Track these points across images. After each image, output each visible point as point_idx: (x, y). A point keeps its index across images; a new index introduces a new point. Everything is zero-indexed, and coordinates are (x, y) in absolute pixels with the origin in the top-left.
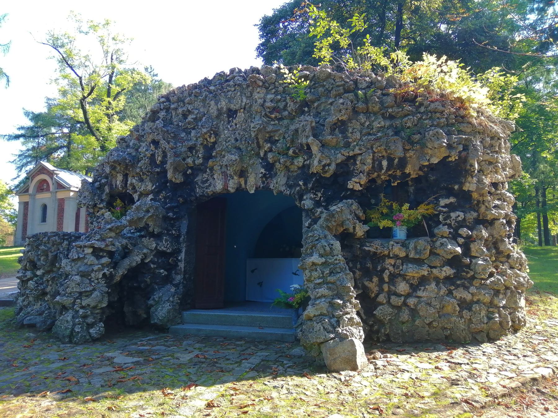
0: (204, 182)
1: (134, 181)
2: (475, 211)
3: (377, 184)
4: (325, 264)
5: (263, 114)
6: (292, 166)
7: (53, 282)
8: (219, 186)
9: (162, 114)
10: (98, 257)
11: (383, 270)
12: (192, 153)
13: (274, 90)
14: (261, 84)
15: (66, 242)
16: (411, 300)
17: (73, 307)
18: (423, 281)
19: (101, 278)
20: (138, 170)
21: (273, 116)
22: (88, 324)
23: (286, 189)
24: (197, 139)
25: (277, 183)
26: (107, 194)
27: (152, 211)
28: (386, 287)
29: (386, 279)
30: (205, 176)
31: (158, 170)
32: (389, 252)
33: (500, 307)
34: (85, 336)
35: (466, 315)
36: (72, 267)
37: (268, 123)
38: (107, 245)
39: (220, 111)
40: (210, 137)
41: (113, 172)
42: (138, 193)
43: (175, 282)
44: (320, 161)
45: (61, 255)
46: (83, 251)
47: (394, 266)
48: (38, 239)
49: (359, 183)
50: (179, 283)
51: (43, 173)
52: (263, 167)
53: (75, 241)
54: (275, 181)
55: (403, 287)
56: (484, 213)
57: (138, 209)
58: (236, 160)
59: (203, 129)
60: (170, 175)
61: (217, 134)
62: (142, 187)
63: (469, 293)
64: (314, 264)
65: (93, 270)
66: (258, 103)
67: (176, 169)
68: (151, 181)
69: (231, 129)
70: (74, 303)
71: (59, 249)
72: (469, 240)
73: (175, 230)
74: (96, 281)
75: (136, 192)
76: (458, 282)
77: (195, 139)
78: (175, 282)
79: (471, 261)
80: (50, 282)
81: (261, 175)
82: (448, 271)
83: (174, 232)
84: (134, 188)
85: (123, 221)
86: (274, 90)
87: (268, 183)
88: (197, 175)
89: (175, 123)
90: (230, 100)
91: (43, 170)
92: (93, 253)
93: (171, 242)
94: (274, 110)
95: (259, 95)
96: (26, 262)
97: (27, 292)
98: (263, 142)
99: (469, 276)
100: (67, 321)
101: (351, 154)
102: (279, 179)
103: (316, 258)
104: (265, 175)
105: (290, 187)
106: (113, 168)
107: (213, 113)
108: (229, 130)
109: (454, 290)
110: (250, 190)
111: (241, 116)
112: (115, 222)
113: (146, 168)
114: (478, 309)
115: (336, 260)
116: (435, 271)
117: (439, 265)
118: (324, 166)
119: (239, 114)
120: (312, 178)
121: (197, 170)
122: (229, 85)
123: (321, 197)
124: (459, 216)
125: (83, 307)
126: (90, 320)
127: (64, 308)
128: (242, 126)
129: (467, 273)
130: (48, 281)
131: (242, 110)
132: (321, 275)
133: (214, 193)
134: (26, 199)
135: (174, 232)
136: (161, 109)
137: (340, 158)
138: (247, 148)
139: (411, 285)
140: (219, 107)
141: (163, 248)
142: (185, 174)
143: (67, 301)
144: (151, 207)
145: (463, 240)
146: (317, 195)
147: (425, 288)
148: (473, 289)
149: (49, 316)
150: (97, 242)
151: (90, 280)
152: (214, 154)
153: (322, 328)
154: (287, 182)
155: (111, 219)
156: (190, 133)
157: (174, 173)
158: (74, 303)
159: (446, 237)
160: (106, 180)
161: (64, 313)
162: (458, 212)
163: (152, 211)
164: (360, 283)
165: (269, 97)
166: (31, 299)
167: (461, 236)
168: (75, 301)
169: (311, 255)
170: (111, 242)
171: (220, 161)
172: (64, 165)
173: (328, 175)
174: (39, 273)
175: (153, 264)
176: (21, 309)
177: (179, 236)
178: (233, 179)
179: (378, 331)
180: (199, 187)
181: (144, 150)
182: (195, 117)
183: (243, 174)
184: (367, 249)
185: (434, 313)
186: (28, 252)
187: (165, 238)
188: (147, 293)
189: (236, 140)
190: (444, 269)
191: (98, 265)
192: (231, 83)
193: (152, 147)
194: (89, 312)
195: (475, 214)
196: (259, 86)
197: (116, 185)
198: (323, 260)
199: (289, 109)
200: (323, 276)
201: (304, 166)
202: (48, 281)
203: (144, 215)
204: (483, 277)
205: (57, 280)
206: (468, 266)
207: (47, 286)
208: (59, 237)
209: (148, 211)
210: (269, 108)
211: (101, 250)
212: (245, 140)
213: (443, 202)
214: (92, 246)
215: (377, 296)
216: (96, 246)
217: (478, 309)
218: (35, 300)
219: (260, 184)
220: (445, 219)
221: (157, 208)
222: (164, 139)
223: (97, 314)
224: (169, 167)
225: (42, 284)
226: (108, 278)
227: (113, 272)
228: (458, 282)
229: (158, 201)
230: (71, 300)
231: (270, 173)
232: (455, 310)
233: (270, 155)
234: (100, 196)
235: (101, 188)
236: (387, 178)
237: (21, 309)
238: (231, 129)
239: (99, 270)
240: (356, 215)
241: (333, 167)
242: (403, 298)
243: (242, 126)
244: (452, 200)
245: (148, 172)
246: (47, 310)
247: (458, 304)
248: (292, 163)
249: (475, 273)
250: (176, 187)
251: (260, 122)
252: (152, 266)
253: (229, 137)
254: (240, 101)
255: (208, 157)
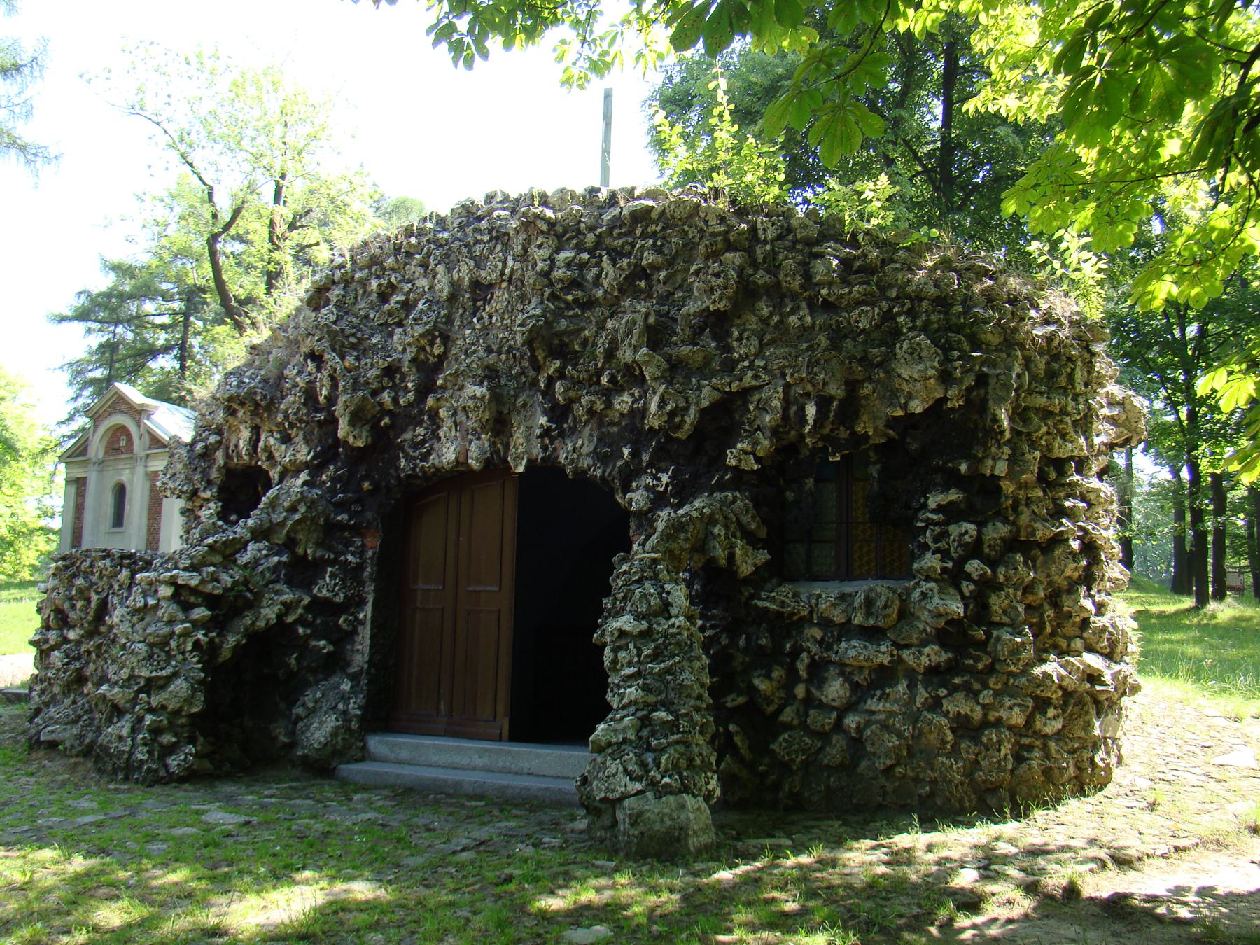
0: (416, 445)
1: (272, 441)
2: (1005, 521)
3: (802, 457)
4: (646, 635)
5: (546, 294)
6: (609, 412)
7: (98, 656)
8: (448, 454)
9: (335, 294)
10: (187, 607)
11: (796, 653)
12: (392, 379)
13: (575, 241)
14: (545, 228)
15: (125, 573)
16: (851, 718)
17: (134, 708)
18: (883, 676)
19: (191, 651)
20: (280, 417)
21: (570, 298)
22: (161, 746)
23: (595, 465)
24: (404, 350)
25: (574, 450)
26: (219, 469)
27: (302, 509)
28: (800, 691)
29: (803, 674)
30: (421, 431)
31: (321, 416)
32: (811, 612)
33: (1046, 736)
34: (156, 771)
35: (968, 752)
36: (133, 626)
37: (558, 314)
38: (203, 581)
39: (455, 285)
40: (432, 344)
41: (231, 419)
42: (279, 468)
43: (352, 670)
44: (662, 403)
45: (116, 600)
46: (156, 591)
47: (821, 643)
48: (73, 564)
49: (753, 453)
50: (361, 672)
51: (121, 411)
52: (545, 413)
53: (142, 570)
54: (570, 447)
55: (835, 690)
56: (1028, 526)
57: (273, 504)
58: (483, 397)
59: (416, 327)
60: (343, 430)
61: (446, 339)
62: (285, 455)
63: (978, 703)
64: (622, 633)
65: (173, 633)
66: (538, 269)
67: (356, 418)
68: (307, 441)
69: (478, 326)
70: (134, 701)
71: (112, 586)
72: (987, 586)
73: (353, 554)
74: (180, 657)
75: (274, 465)
76: (957, 681)
77: (400, 349)
78: (352, 670)
79: (988, 635)
80: (94, 655)
81: (538, 432)
82: (933, 655)
83: (350, 558)
84: (271, 457)
85: (239, 530)
86: (575, 241)
87: (555, 449)
88: (403, 431)
89: (362, 313)
90: (480, 262)
91: (121, 403)
92: (175, 597)
93: (344, 580)
94: (575, 284)
95: (541, 252)
96: (48, 612)
97: (49, 675)
98: (545, 358)
99: (980, 666)
100: (120, 738)
101: (735, 386)
102: (580, 442)
103: (625, 622)
104: (546, 433)
105: (604, 459)
106: (231, 412)
107: (441, 291)
108: (474, 329)
109: (945, 697)
110: (516, 466)
111: (501, 298)
112: (224, 531)
113: (295, 414)
114: (995, 739)
115: (673, 626)
116: (907, 655)
117: (915, 642)
118: (672, 414)
119: (498, 293)
120: (651, 441)
121: (405, 418)
122: (478, 230)
123: (667, 485)
124: (966, 532)
125: (151, 710)
126: (167, 739)
127: (117, 711)
128: (503, 319)
129: (978, 659)
130: (89, 653)
131: (504, 285)
132: (636, 659)
133: (438, 470)
134: (78, 473)
135: (350, 558)
136: (334, 283)
137: (707, 396)
138: (511, 368)
139: (855, 687)
140: (456, 277)
141: (324, 591)
142: (375, 429)
143: (115, 694)
144: (299, 501)
145: (972, 587)
146: (659, 479)
147: (884, 693)
148: (986, 697)
149: (90, 725)
150: (182, 573)
151: (168, 653)
152: (440, 382)
153: (621, 769)
154: (596, 448)
155: (214, 523)
156: (391, 335)
157: (352, 423)
158: (134, 701)
159: (935, 581)
160: (218, 438)
161: (115, 720)
162: (965, 524)
163: (302, 509)
164: (743, 681)
165: (565, 255)
166: (56, 690)
167: (968, 577)
168: (136, 697)
169: (618, 614)
170: (213, 573)
171: (452, 397)
172: (163, 392)
173: (681, 435)
174: (72, 635)
175: (303, 626)
176: (38, 712)
177: (360, 567)
178: (479, 439)
179: (777, 787)
180: (407, 456)
181: (295, 372)
182: (403, 298)
183: (500, 426)
184: (760, 604)
185: (898, 747)
186: (54, 589)
187: (329, 569)
188: (293, 687)
189: (489, 350)
190: (927, 650)
191: (183, 622)
192: (484, 224)
193: (311, 366)
194: (166, 722)
195: (1004, 530)
196: (542, 232)
197: (237, 446)
198: (644, 625)
199: (605, 283)
200: (639, 662)
201: (632, 411)
202: (89, 653)
203: (286, 519)
204: (1012, 668)
205: (106, 651)
206: (982, 645)
207: (88, 663)
208: (112, 560)
209: (293, 509)
210: (561, 280)
211: (194, 591)
212: (509, 352)
213: (934, 500)
214: (172, 582)
215: (780, 710)
216: (180, 582)
217: (995, 739)
218: (64, 693)
219: (537, 452)
220: (937, 539)
221: (313, 502)
222: (334, 350)
223: (182, 726)
224: (342, 411)
225: (78, 658)
226: (208, 653)
227: (217, 640)
228: (957, 681)
229: (319, 487)
230: (130, 693)
231: (559, 428)
232: (944, 742)
233: (559, 387)
234: (205, 473)
235: (207, 454)
236: (820, 444)
237: (38, 712)
238: (478, 326)
239: (186, 634)
240: (741, 526)
241: (691, 418)
242: (835, 715)
243: (503, 319)
244: (954, 495)
245: (301, 421)
246: (86, 712)
247: (951, 728)
248: (609, 405)
249: (996, 660)
250: (357, 457)
251: (538, 312)
252: (301, 630)
253: (473, 344)
254: (500, 264)
255: (426, 389)
